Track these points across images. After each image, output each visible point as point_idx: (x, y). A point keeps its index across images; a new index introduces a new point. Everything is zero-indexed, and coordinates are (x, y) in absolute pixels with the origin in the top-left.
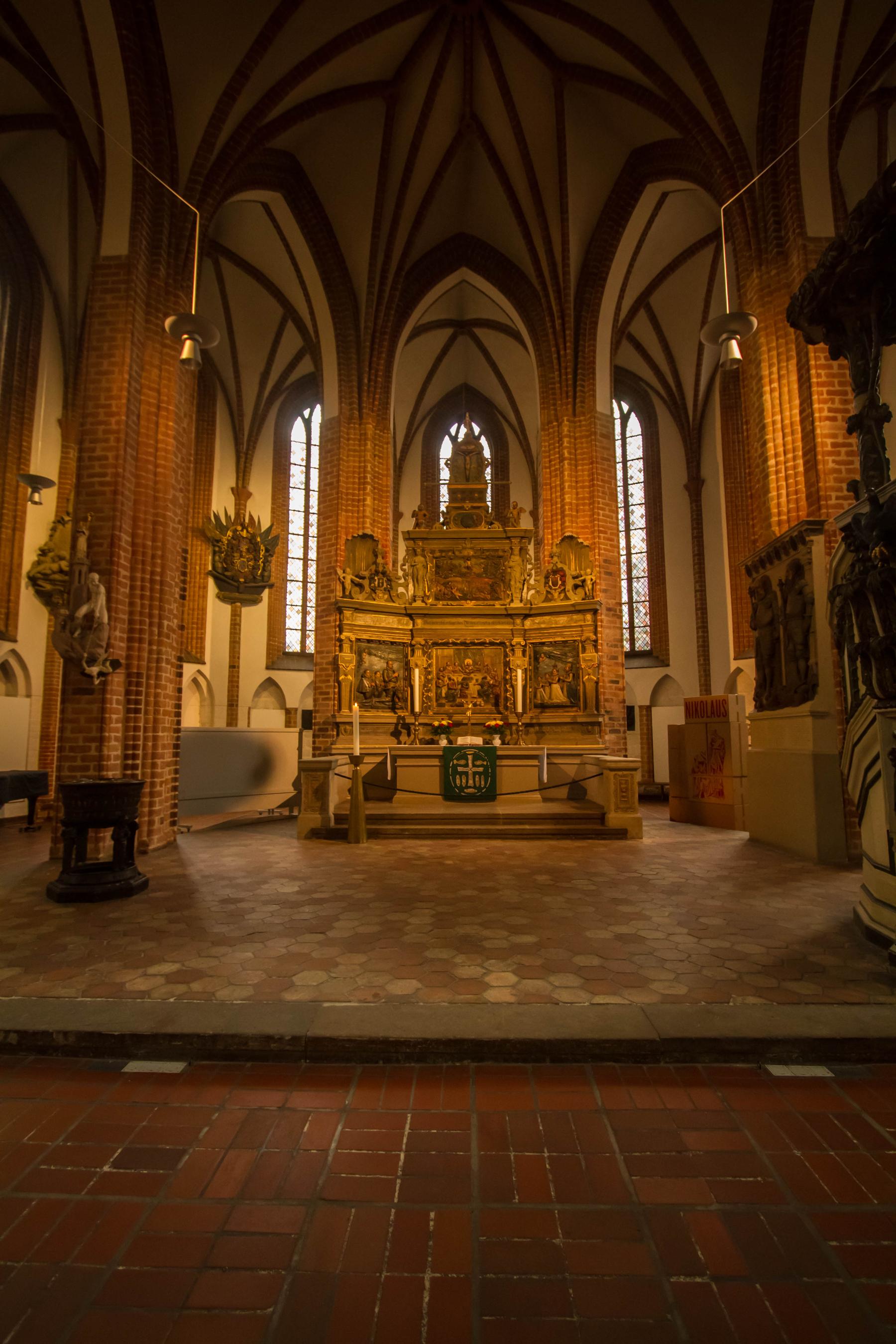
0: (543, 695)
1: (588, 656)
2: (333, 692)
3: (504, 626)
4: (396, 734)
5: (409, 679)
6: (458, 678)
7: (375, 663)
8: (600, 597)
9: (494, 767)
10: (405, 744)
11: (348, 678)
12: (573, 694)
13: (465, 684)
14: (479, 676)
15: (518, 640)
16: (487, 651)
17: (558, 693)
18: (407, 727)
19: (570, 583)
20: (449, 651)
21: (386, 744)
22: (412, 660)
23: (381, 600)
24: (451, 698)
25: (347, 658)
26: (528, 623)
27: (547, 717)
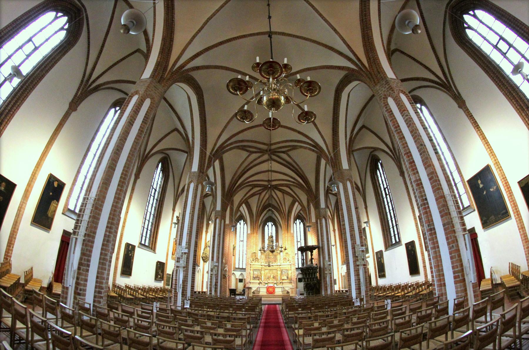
0: (283, 278)
1: (290, 272)
2: (249, 277)
3: (277, 267)
4: (259, 284)
5: (261, 275)
6: (269, 275)
7: (256, 273)
8: (292, 262)
9: (274, 289)
10: (261, 286)
11: (252, 275)
12: (288, 278)
13: (270, 276)
14: (272, 275)
15: (279, 269)
16: (274, 271)
17: (286, 278)
18: (261, 283)
19: (287, 260)
20: (268, 271)
21: (258, 286)
22: (262, 272)
23: (257, 263)
24: (268, 278)
25: (252, 272)
26: (281, 266)
27: (284, 281)
